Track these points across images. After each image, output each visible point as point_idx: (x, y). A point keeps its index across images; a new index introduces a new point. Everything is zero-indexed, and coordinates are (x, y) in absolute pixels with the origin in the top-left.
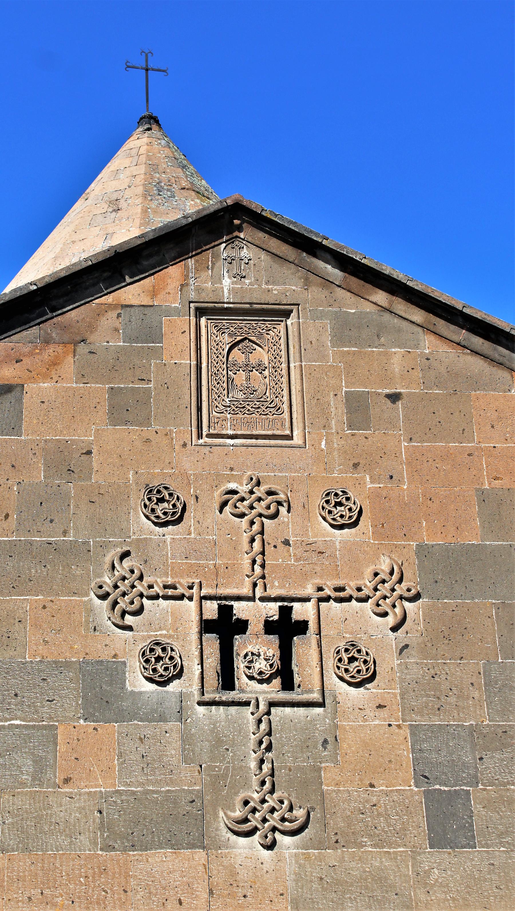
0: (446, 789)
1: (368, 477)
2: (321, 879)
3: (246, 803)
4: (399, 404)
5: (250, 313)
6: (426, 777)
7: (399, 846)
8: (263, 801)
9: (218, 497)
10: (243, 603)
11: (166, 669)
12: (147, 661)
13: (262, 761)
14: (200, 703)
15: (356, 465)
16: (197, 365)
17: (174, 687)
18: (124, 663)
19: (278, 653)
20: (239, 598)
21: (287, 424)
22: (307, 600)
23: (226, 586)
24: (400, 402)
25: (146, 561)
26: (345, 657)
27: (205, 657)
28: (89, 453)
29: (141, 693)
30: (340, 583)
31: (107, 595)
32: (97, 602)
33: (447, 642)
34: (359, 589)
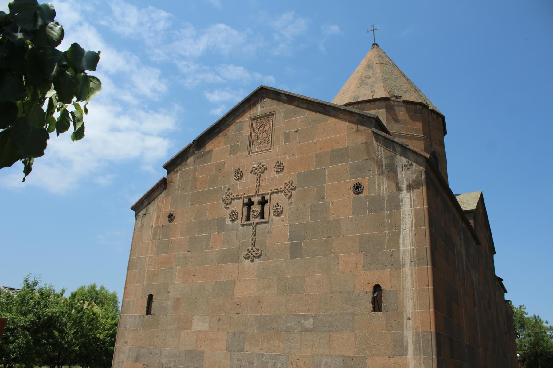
0: (296, 242)
3: (248, 250)
4: (298, 133)
5: (383, 99)
6: (292, 239)
7: (283, 259)
8: (252, 249)
9: (251, 169)
11: (234, 217)
12: (231, 216)
13: (253, 239)
15: (285, 153)
17: (236, 222)
18: (226, 217)
19: (260, 210)
21: (270, 146)
22: (268, 194)
23: (250, 193)
24: (298, 132)
26: (275, 208)
27: (243, 213)
28: (224, 164)
29: (229, 224)
30: (276, 188)
31: (224, 200)
32: (284, 197)
33: (301, 200)
34: (281, 189)
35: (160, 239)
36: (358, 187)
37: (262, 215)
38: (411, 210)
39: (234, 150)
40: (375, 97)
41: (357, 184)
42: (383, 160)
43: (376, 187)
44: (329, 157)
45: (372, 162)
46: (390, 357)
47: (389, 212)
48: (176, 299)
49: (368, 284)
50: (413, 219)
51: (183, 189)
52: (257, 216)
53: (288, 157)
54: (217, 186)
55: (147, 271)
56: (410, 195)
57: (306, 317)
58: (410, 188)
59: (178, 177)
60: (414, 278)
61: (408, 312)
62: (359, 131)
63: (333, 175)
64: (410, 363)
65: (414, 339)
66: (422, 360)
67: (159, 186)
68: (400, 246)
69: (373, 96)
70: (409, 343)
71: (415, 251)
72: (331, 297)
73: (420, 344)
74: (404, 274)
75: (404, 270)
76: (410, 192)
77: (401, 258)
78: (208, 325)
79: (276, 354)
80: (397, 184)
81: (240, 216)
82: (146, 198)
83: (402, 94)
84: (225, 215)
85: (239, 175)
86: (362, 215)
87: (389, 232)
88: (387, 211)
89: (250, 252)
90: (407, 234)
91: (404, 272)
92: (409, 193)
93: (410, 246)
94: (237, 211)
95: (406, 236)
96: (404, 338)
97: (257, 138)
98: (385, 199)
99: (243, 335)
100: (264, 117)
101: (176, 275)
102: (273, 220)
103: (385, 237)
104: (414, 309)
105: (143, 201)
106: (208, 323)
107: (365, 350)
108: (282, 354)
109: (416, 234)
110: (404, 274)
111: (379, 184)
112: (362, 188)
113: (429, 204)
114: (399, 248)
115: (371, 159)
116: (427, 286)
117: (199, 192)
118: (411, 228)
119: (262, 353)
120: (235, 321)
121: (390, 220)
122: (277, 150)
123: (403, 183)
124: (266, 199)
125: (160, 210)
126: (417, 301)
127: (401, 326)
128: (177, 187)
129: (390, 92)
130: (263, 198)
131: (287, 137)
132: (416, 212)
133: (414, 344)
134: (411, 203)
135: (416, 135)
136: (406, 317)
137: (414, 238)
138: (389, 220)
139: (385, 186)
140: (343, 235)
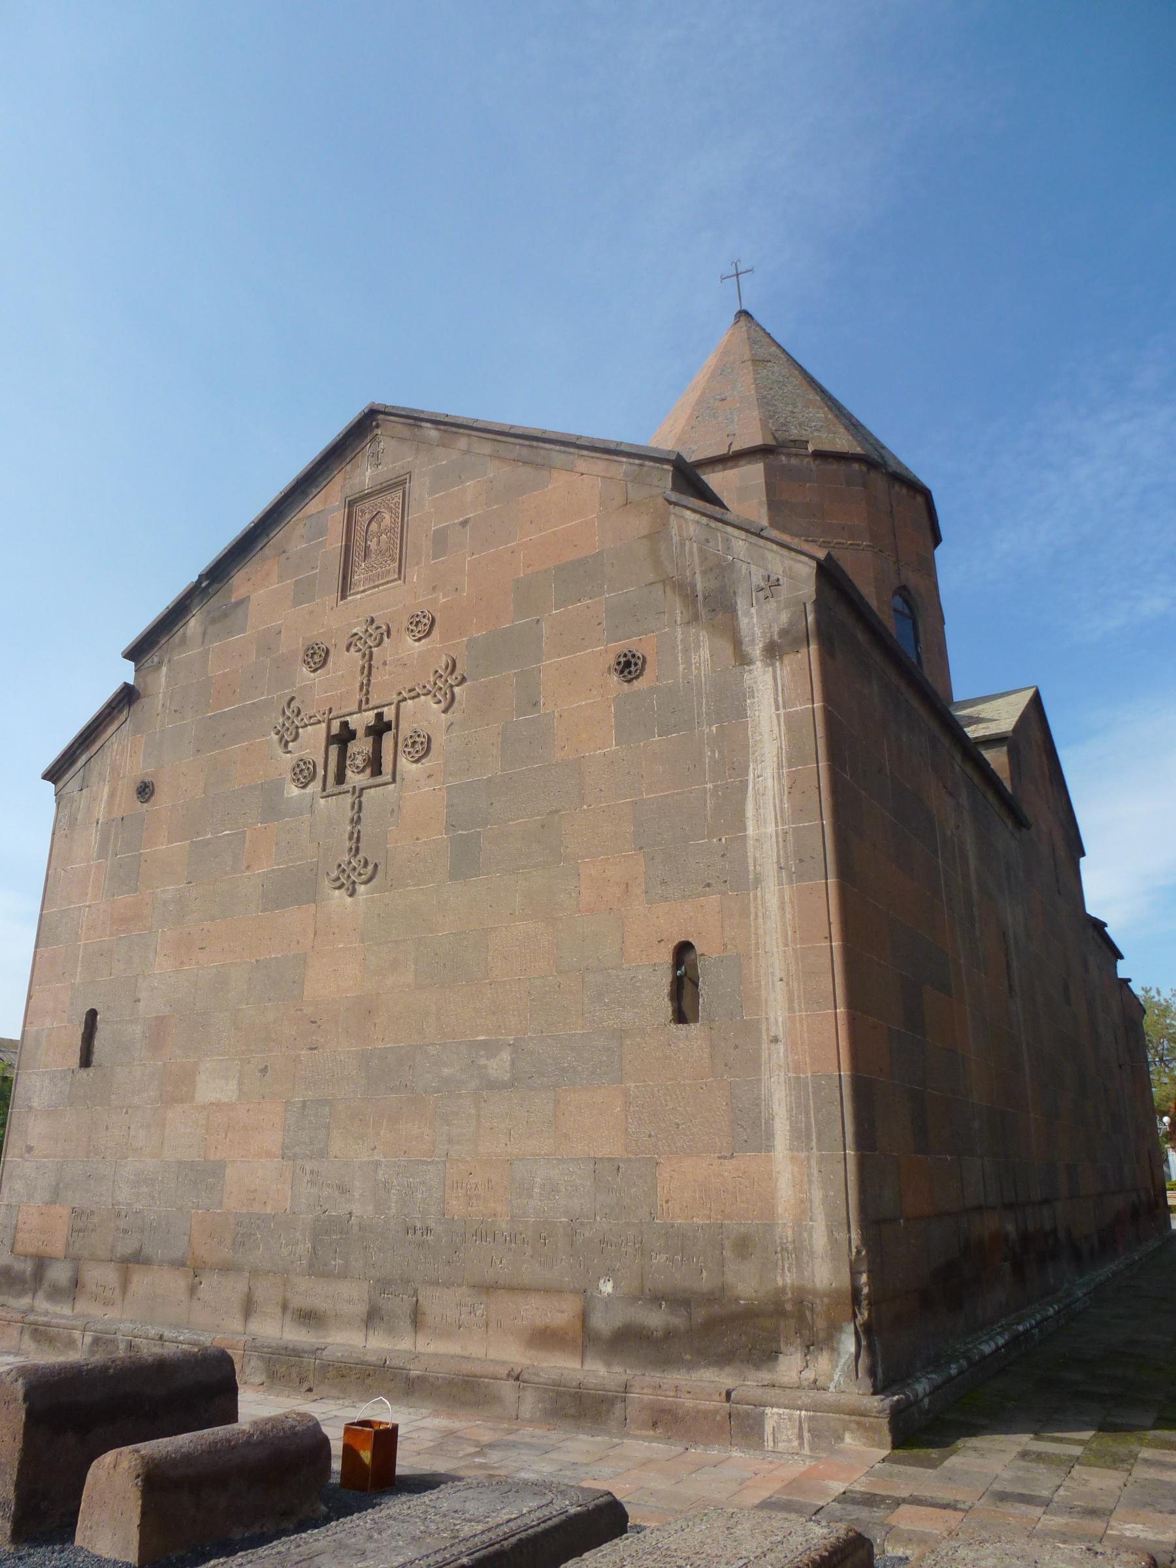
1: (441, 594)
2: (379, 915)
7: (430, 883)
10: (355, 716)
12: (295, 774)
14: (322, 798)
16: (346, 545)
18: (285, 778)
19: (371, 751)
20: (351, 714)
21: (397, 570)
25: (303, 701)
26: (410, 742)
28: (280, 632)
35: (116, 855)
36: (628, 664)
37: (375, 764)
38: (778, 716)
39: (303, 593)
40: (735, 448)
41: (625, 655)
42: (698, 577)
43: (680, 658)
44: (551, 586)
45: (668, 589)
46: (725, 1158)
47: (714, 729)
48: (157, 1018)
49: (659, 942)
50: (784, 743)
51: (175, 711)
52: (364, 768)
53: (443, 598)
54: (262, 694)
55: (85, 944)
56: (774, 672)
57: (491, 1048)
58: (773, 652)
59: (163, 679)
60: (788, 916)
61: (772, 1019)
62: (630, 503)
63: (561, 634)
64: (778, 1173)
65: (791, 1102)
66: (813, 1162)
67: (114, 708)
68: (748, 824)
69: (731, 444)
70: (777, 1114)
71: (790, 838)
72: (559, 986)
73: (807, 1113)
74: (760, 908)
75: (759, 894)
76: (773, 665)
77: (751, 861)
78: (235, 1087)
79: (411, 1161)
80: (737, 643)
81: (320, 772)
82: (81, 744)
83: (811, 435)
84: (280, 775)
85: (318, 657)
86: (642, 744)
87: (714, 786)
88: (710, 726)
89: (344, 871)
90: (766, 787)
91: (760, 902)
92: (771, 668)
93: (776, 823)
94: (310, 758)
95: (763, 794)
96: (763, 1098)
97: (363, 554)
98: (704, 691)
99: (327, 1109)
100: (380, 491)
101: (156, 953)
102: (405, 776)
103: (705, 801)
104: (789, 1009)
105: (74, 752)
106: (235, 1082)
107: (654, 1139)
108: (429, 1160)
109: (791, 788)
110: (760, 908)
111: (686, 651)
112: (640, 666)
113: (827, 697)
114: (745, 830)
115: (663, 581)
116: (826, 938)
117: (214, 716)
118: (779, 769)
119: (377, 1158)
120: (306, 1070)
121: (719, 752)
122: (415, 580)
123: (754, 640)
124: (386, 719)
125: (119, 775)
126: (799, 986)
127: (753, 1063)
128: (160, 707)
129: (776, 430)
130: (379, 716)
131: (440, 541)
132: (792, 724)
133: (791, 1116)
134: (778, 696)
135: (851, 544)
136: (768, 1035)
137: (785, 798)
138: (717, 752)
139: (702, 652)
140: (590, 806)
